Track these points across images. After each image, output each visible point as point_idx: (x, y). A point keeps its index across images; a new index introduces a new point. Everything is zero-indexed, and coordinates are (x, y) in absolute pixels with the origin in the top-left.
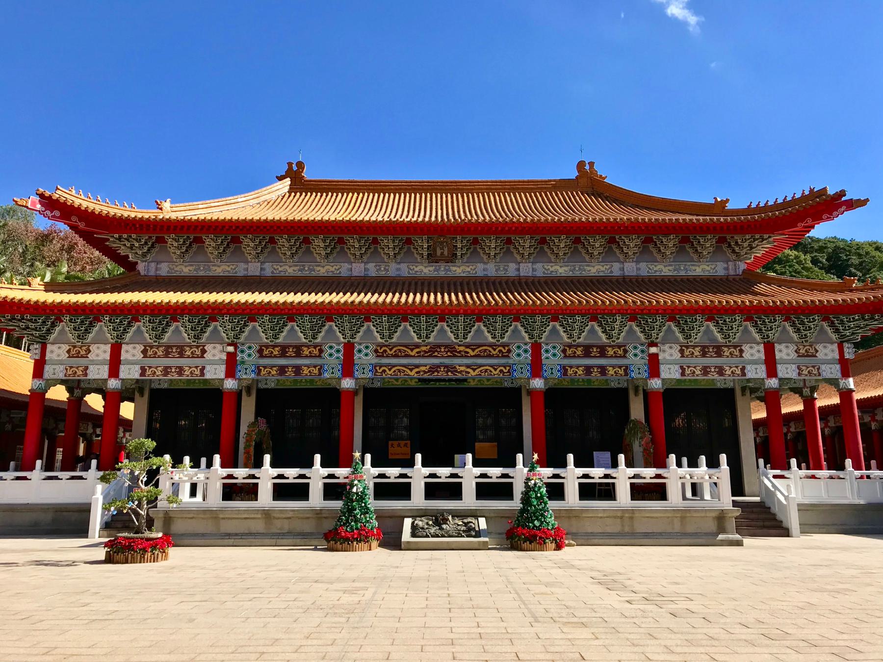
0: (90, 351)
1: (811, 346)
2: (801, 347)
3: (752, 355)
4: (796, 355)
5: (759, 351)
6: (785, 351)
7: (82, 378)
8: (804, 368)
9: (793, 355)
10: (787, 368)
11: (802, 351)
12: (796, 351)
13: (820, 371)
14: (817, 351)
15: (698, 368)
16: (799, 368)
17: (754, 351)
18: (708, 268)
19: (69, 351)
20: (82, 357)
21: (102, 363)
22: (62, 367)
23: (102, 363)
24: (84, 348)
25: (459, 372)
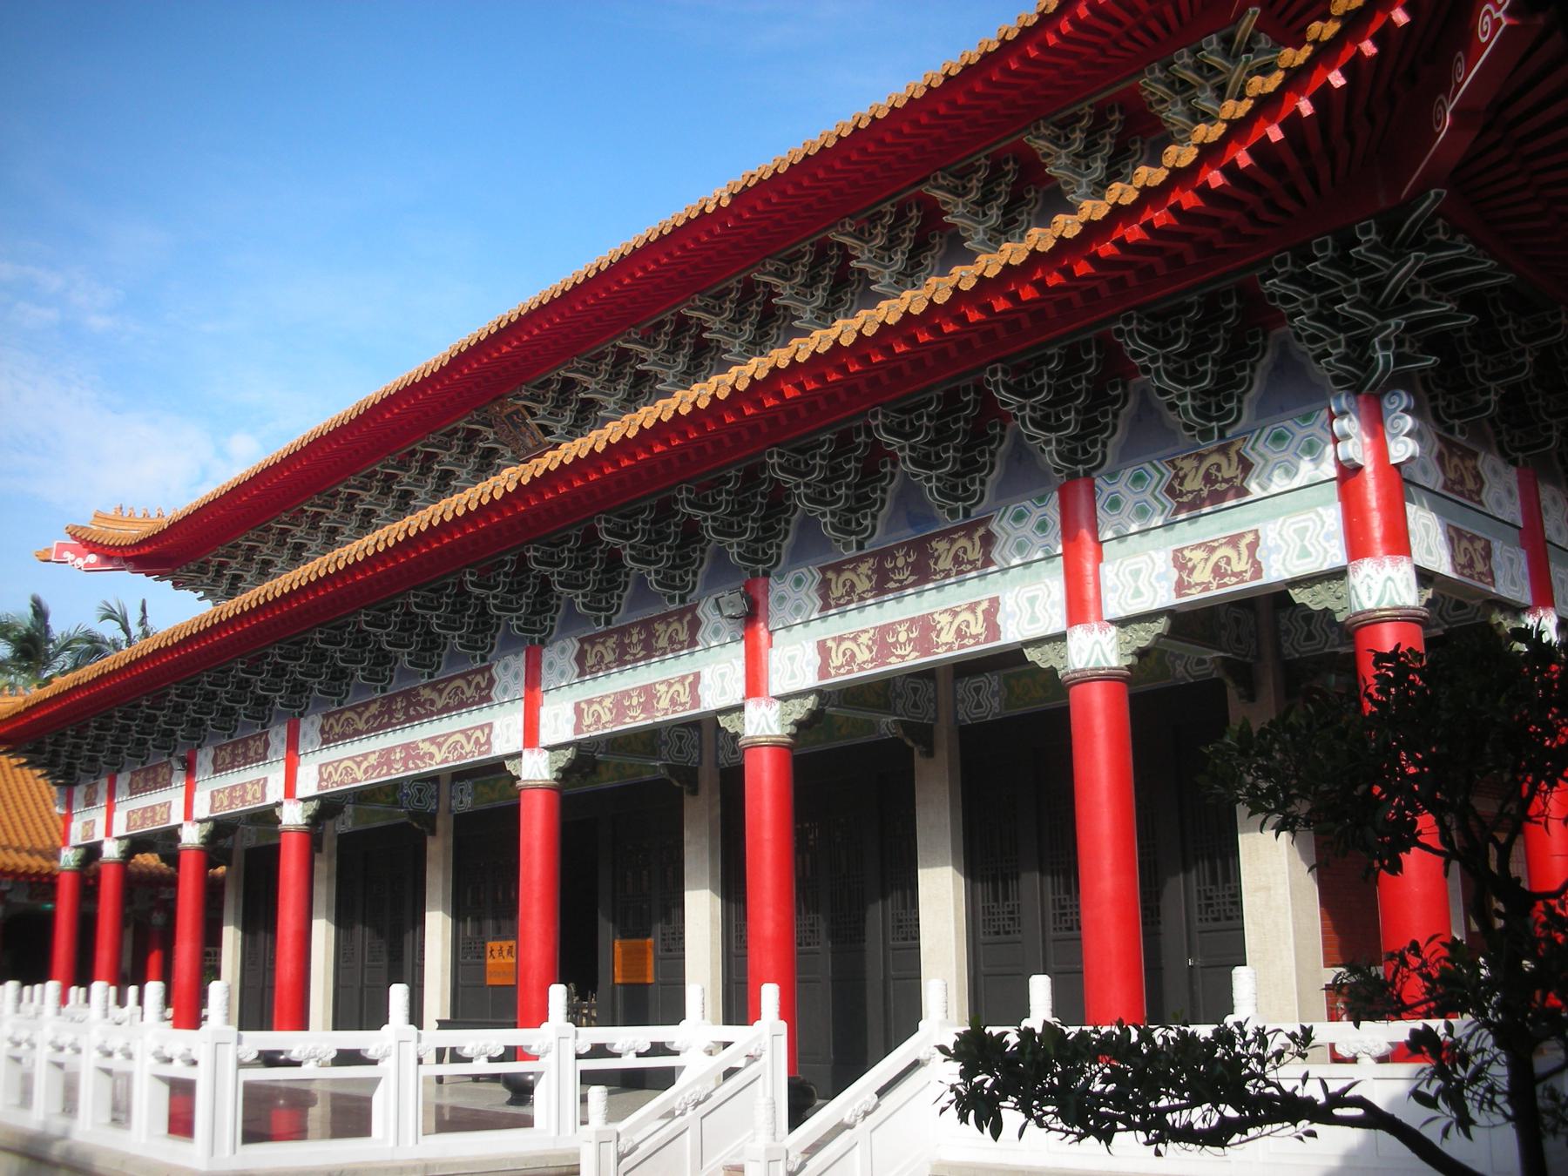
1: (1223, 450)
2: (1187, 465)
5: (1042, 526)
8: (1198, 555)
12: (1170, 491)
13: (1260, 554)
15: (864, 639)
25: (421, 758)
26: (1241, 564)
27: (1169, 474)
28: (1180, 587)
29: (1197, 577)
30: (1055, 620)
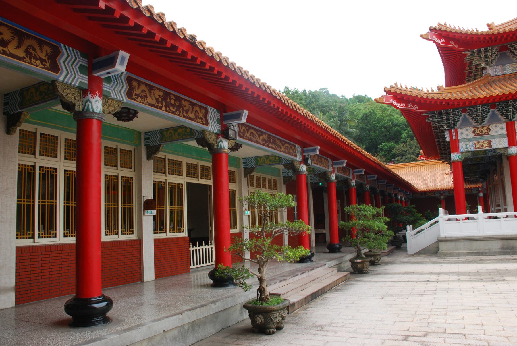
0: (490, 130)
7: (488, 148)
19: (474, 132)
20: (485, 134)
21: (502, 136)
22: (471, 143)
23: (502, 136)
24: (485, 128)
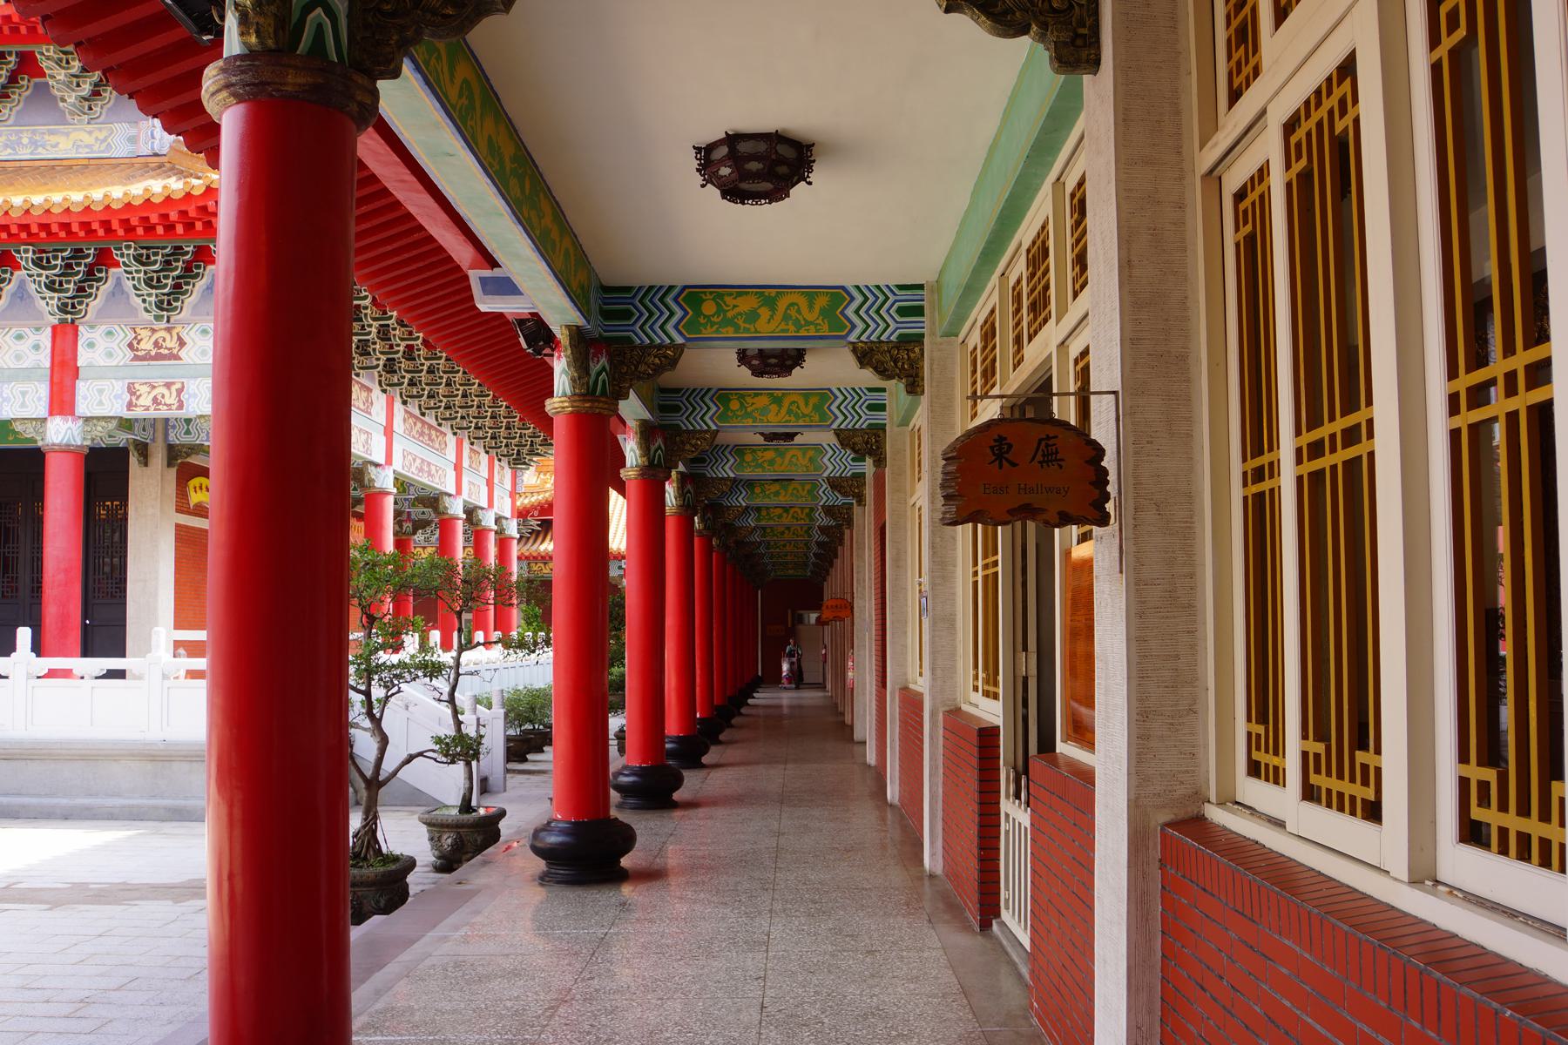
1: (169, 330)
2: (144, 334)
3: (18, 358)
4: (130, 354)
5: (37, 347)
6: (102, 343)
8: (143, 389)
9: (123, 356)
10: (101, 392)
11: (147, 345)
12: (130, 346)
13: (184, 396)
14: (182, 343)
16: (131, 390)
17: (25, 346)
18: (88, 139)
26: (171, 399)
27: (131, 336)
28: (130, 406)
29: (141, 401)
30: (41, 410)
